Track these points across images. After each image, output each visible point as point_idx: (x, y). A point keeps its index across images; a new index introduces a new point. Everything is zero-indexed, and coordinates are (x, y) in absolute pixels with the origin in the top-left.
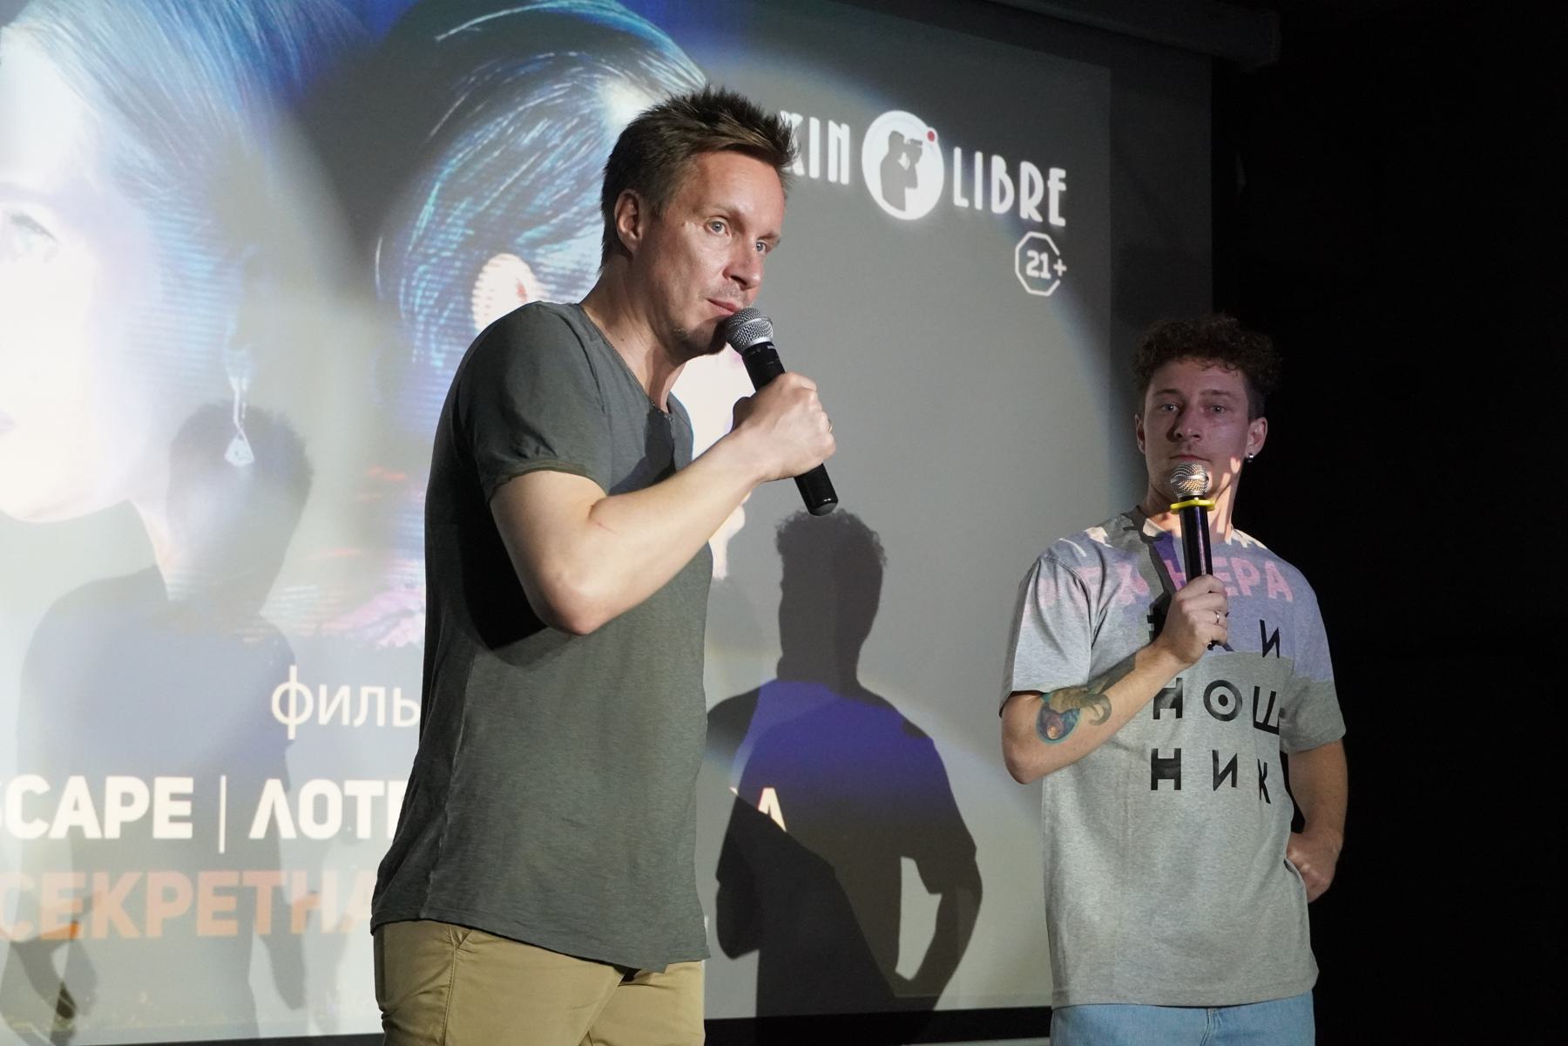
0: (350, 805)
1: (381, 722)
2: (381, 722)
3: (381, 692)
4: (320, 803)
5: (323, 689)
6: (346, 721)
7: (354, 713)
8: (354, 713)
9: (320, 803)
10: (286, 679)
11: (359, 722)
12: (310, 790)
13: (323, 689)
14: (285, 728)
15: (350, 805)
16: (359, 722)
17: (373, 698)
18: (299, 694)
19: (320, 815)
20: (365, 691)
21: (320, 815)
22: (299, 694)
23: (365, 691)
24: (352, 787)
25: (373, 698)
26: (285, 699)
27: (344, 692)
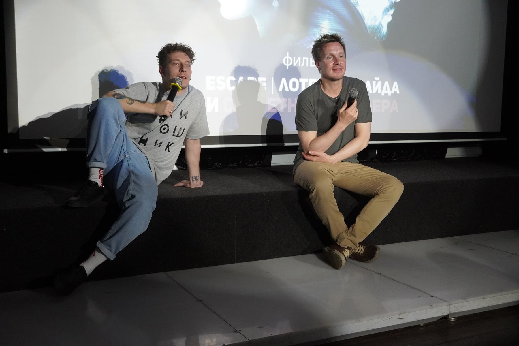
0: (300, 84)
1: (307, 65)
2: (307, 65)
3: (307, 59)
4: (294, 83)
5: (294, 58)
6: (299, 65)
7: (301, 63)
8: (301, 63)
9: (294, 83)
10: (286, 55)
11: (302, 65)
12: (292, 80)
13: (294, 58)
14: (286, 66)
15: (300, 84)
16: (302, 65)
17: (305, 60)
18: (289, 59)
19: (294, 86)
20: (304, 58)
21: (294, 86)
22: (289, 59)
23: (304, 58)
24: (301, 80)
25: (305, 60)
26: (286, 59)
27: (299, 58)
